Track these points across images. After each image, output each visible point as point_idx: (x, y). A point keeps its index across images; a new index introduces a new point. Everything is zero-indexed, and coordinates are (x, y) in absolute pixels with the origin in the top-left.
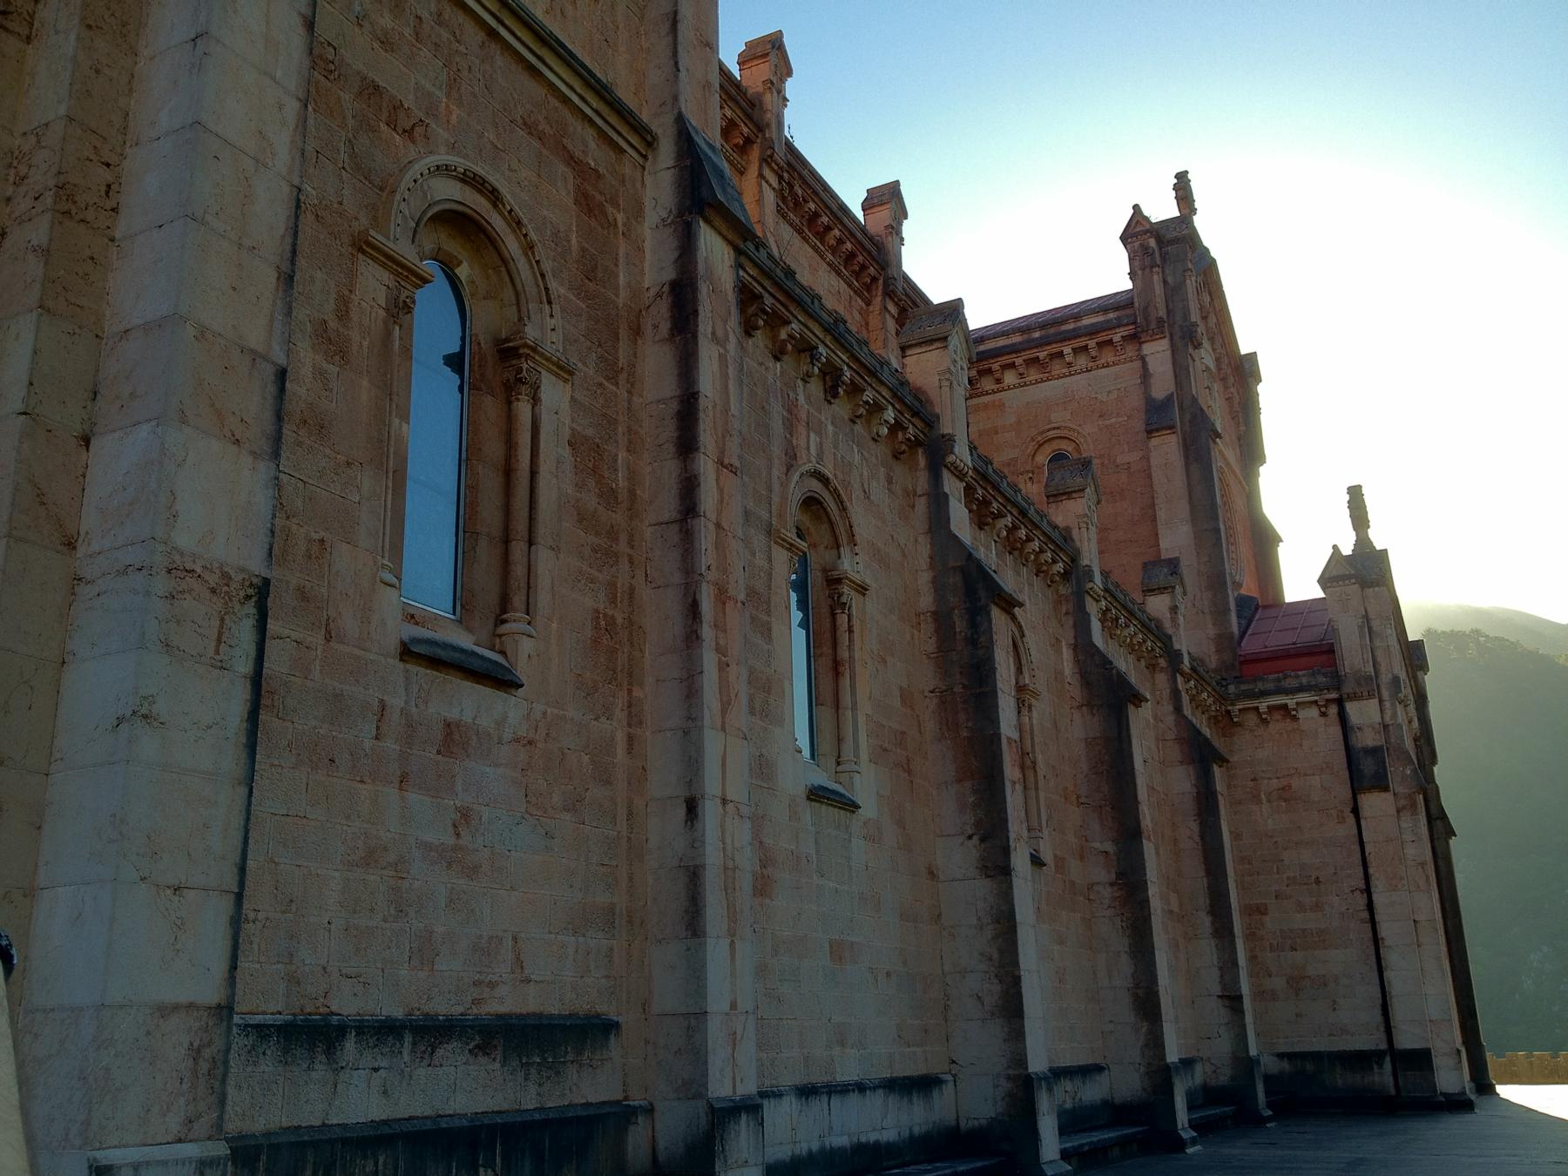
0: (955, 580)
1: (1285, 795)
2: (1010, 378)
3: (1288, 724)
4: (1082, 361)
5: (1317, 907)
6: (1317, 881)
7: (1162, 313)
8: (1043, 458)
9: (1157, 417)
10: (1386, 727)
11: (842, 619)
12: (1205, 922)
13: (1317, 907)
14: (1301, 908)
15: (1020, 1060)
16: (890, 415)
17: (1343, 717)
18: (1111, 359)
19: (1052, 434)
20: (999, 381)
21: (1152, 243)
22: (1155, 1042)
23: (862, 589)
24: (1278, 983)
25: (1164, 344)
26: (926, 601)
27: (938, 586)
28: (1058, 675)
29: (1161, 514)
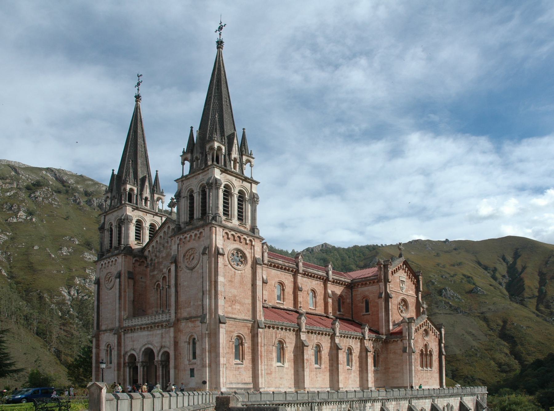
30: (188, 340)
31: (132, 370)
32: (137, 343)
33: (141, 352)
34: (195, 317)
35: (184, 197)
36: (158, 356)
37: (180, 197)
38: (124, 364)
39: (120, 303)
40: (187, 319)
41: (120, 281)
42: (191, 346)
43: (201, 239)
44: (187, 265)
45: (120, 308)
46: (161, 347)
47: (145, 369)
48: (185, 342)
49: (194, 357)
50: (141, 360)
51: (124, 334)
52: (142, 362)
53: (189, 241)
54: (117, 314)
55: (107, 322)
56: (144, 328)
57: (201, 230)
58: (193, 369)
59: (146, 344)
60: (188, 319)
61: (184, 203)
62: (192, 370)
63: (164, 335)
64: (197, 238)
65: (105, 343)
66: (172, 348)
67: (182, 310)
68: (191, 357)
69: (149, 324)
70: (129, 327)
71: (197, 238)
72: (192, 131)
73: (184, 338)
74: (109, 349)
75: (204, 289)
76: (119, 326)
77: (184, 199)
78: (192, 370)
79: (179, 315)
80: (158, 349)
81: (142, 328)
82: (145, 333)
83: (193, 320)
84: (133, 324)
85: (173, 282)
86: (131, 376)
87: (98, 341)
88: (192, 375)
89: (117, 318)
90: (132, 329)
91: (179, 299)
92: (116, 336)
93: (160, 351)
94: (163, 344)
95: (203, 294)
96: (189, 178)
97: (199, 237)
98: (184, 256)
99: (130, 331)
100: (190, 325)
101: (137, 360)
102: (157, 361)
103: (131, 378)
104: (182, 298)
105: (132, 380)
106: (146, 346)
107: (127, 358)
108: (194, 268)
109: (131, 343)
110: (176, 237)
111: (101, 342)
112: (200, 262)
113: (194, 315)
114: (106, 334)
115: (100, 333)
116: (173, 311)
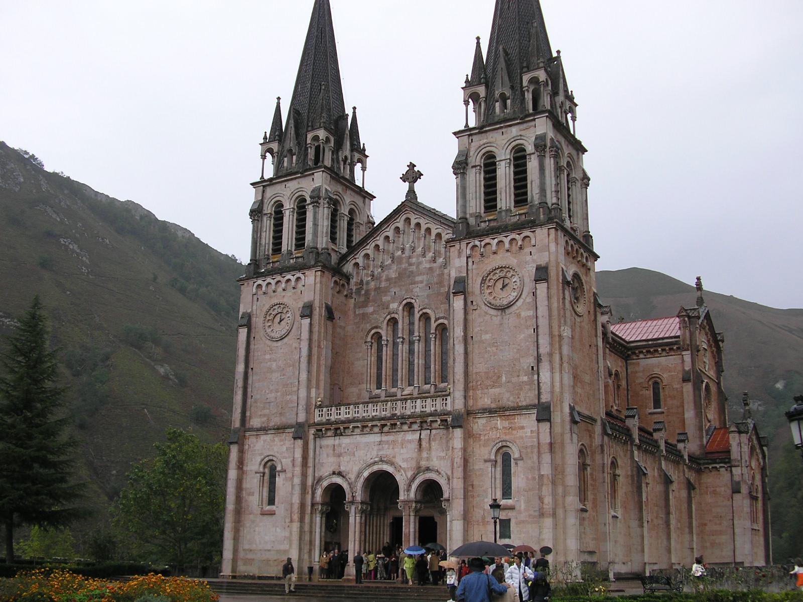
0: (635, 469)
1: (714, 493)
2: (641, 356)
3: (718, 473)
4: (664, 354)
5: (720, 524)
6: (721, 517)
7: (688, 342)
8: (650, 383)
9: (685, 380)
10: (742, 474)
11: (616, 482)
12: (687, 530)
13: (720, 524)
14: (716, 524)
15: (644, 560)
16: (624, 438)
17: (731, 471)
18: (673, 354)
19: (654, 375)
20: (638, 356)
21: (686, 319)
22: (670, 558)
23: (619, 476)
24: (708, 544)
25: (689, 352)
26: (629, 473)
27: (632, 471)
28: (654, 476)
29: (686, 407)
30: (493, 457)
31: (324, 519)
32: (352, 459)
33: (362, 480)
34: (514, 409)
35: (475, 166)
36: (408, 490)
37: (467, 165)
38: (313, 505)
39: (309, 372)
40: (491, 412)
41: (311, 324)
42: (499, 469)
43: (527, 250)
44: (490, 298)
45: (309, 380)
46: (419, 470)
47: (363, 518)
48: (486, 461)
49: (507, 493)
50: (359, 499)
51: (315, 438)
52: (362, 503)
53: (495, 253)
54: (303, 393)
55: (267, 411)
56: (373, 426)
57: (527, 233)
58: (510, 519)
59: (375, 463)
60: (496, 412)
61: (475, 178)
63: (424, 444)
64: (515, 248)
65: (259, 459)
66: (459, 472)
67: (479, 392)
68: (499, 495)
69: (383, 419)
70: (329, 422)
71: (515, 248)
72: (478, 44)
73: (484, 452)
74: (267, 471)
75: (541, 350)
76: (307, 421)
77: (474, 169)
79: (471, 402)
80: (410, 474)
81: (364, 425)
82: (375, 438)
83: (507, 413)
84: (343, 417)
85: (458, 332)
86: (323, 534)
87: (241, 451)
89: (303, 403)
90: (339, 429)
91: (470, 368)
92: (299, 443)
93: (414, 478)
94: (424, 464)
95: (539, 359)
96: (486, 131)
97: (521, 248)
98: (483, 281)
99: (329, 433)
100: (499, 423)
101: (348, 497)
102: (406, 502)
103: (323, 539)
104: (479, 366)
105: (323, 543)
106: (376, 468)
107: (319, 492)
108: (509, 306)
109: (332, 459)
110: (464, 244)
111: (248, 456)
112: (523, 296)
113: (511, 404)
114: (263, 437)
115: (247, 434)
116: (458, 394)
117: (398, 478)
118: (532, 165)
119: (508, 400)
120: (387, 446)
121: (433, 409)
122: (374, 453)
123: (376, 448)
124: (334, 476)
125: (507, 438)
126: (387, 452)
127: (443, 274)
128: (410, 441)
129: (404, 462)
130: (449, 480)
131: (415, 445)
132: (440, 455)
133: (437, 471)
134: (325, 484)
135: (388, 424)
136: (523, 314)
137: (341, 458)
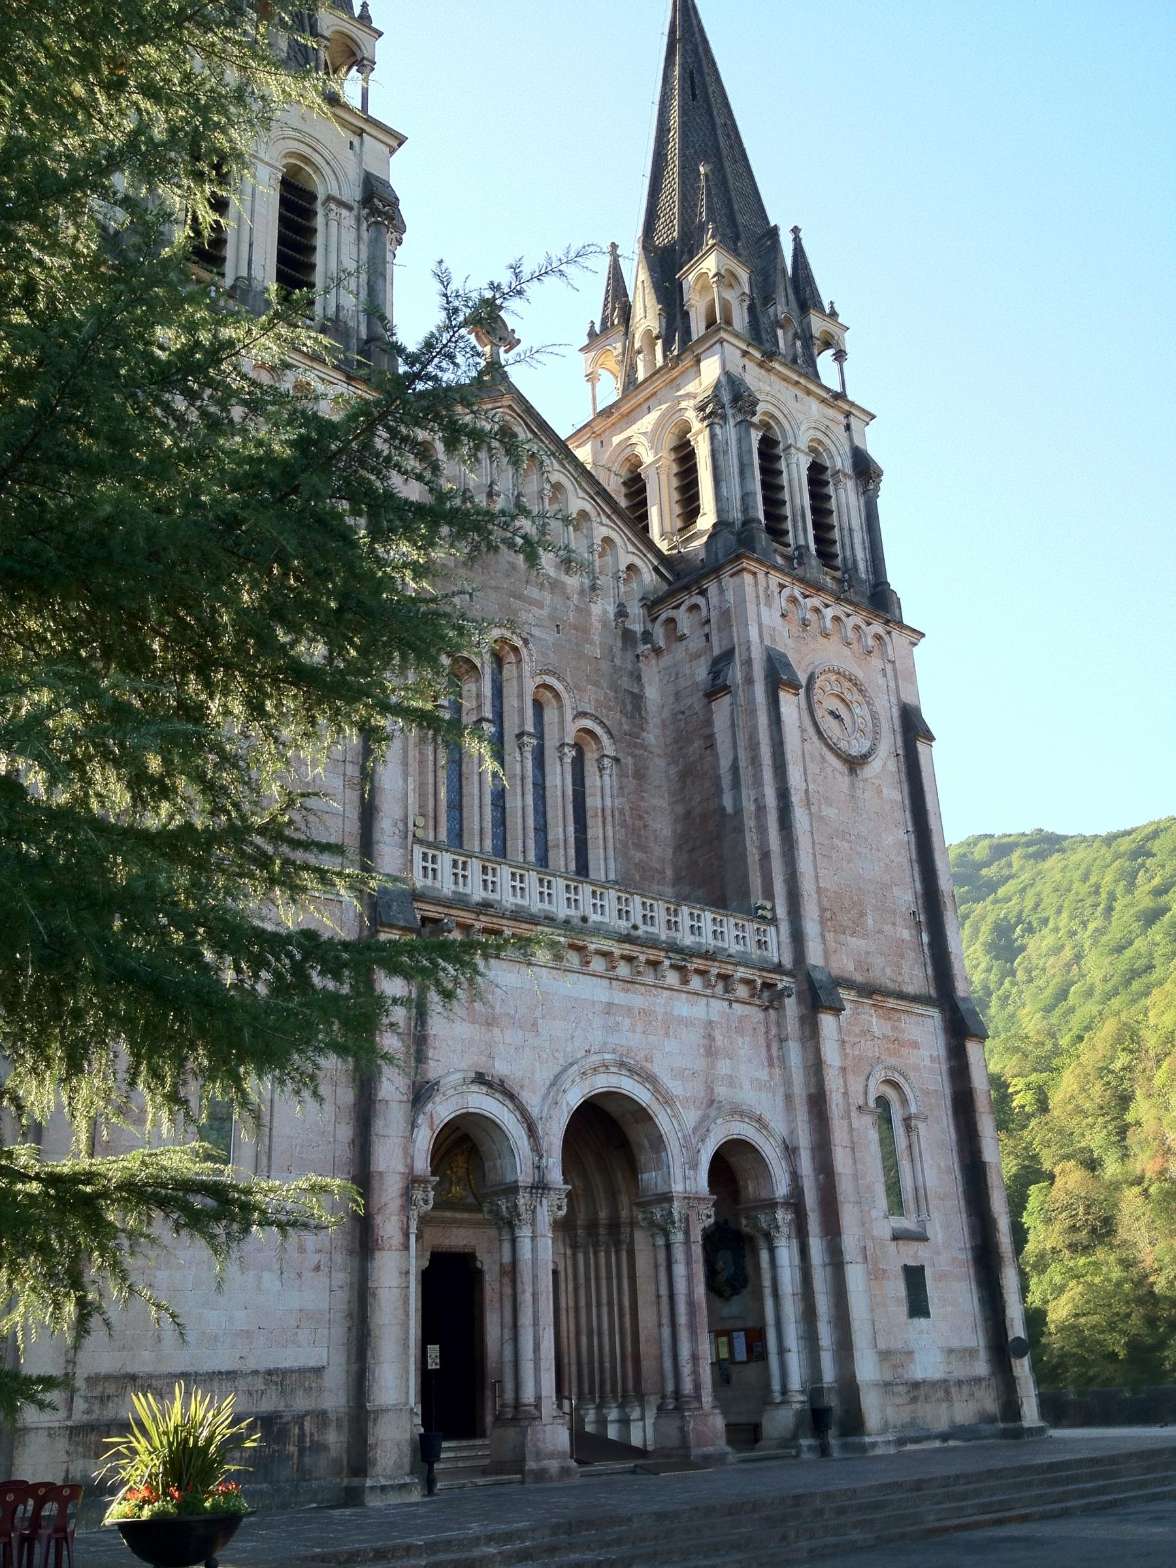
36: (694, 1166)
40: (869, 991)
43: (876, 662)
58: (921, 1269)
62: (914, 1277)
78: (914, 1277)
80: (691, 1117)
82: (594, 990)
83: (891, 1003)
88: (918, 1306)
93: (702, 1129)
94: (722, 1092)
100: (876, 1023)
102: (691, 1199)
106: (602, 1083)
107: (424, 1139)
117: (663, 1121)
118: (845, 497)
119: (883, 970)
120: (627, 1022)
121: (740, 948)
122: (596, 1038)
123: (598, 1022)
124: (475, 1088)
125: (892, 1061)
126: (631, 1039)
127: (588, 613)
128: (688, 1023)
129: (674, 1077)
130: (790, 1151)
131: (694, 1037)
132: (757, 1075)
133: (759, 1120)
134: (443, 1110)
135: (642, 958)
136: (885, 791)
137: (496, 1030)
